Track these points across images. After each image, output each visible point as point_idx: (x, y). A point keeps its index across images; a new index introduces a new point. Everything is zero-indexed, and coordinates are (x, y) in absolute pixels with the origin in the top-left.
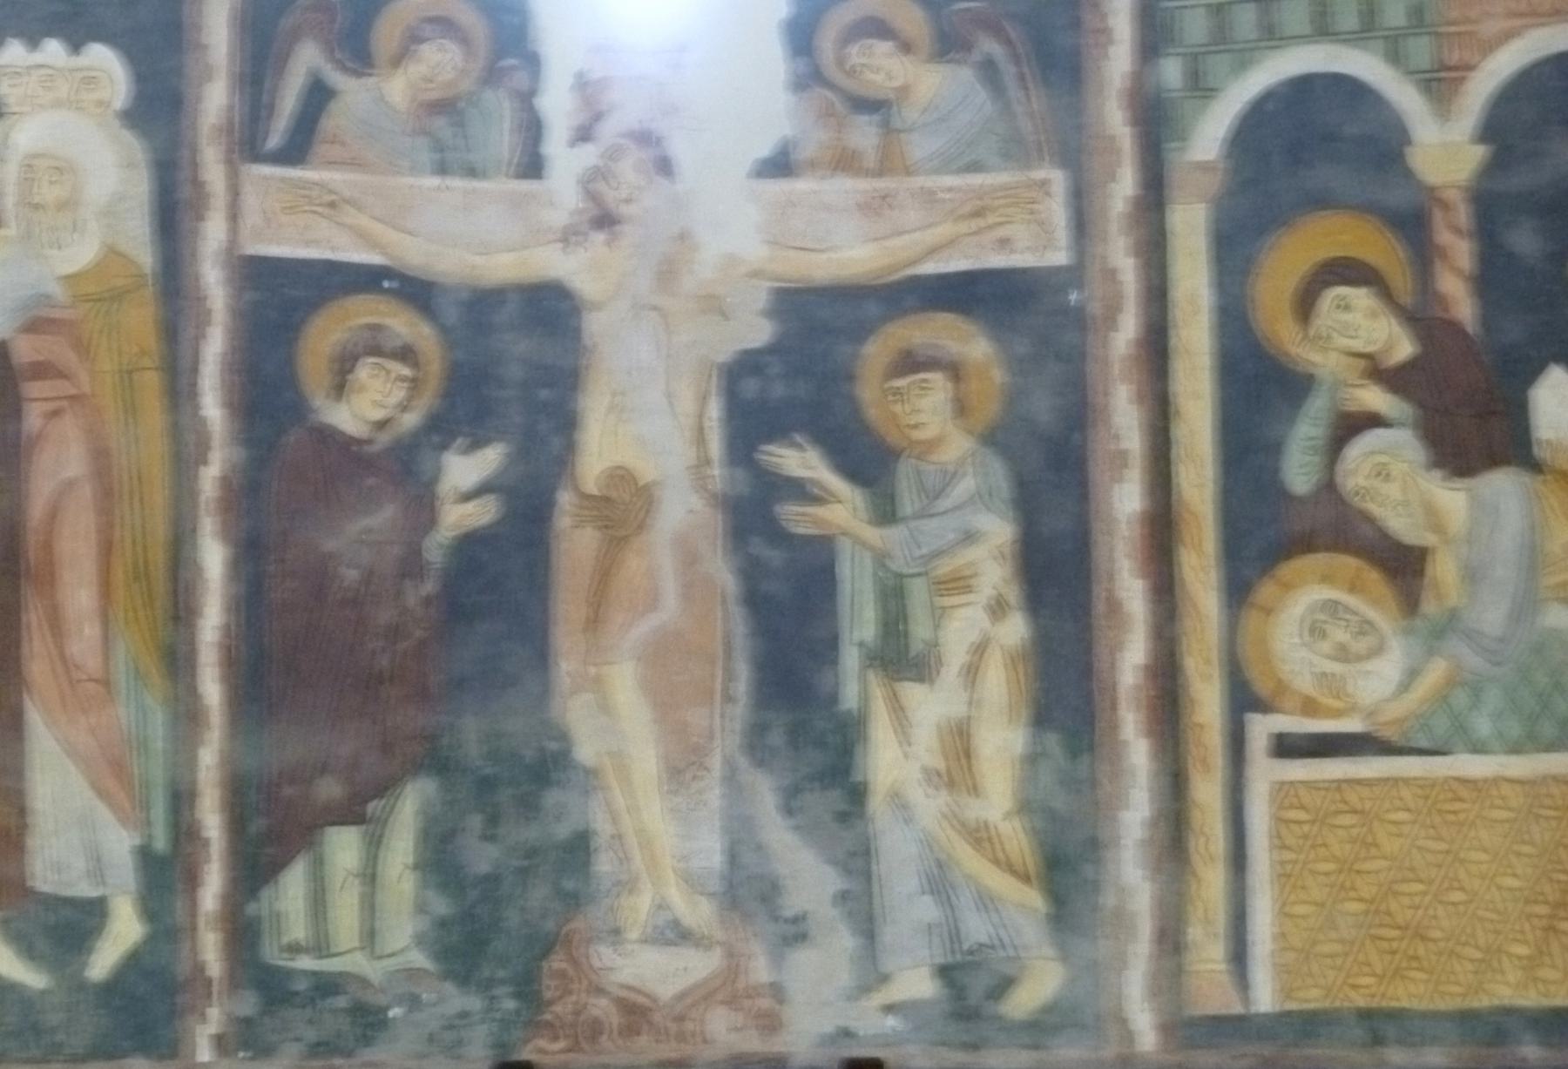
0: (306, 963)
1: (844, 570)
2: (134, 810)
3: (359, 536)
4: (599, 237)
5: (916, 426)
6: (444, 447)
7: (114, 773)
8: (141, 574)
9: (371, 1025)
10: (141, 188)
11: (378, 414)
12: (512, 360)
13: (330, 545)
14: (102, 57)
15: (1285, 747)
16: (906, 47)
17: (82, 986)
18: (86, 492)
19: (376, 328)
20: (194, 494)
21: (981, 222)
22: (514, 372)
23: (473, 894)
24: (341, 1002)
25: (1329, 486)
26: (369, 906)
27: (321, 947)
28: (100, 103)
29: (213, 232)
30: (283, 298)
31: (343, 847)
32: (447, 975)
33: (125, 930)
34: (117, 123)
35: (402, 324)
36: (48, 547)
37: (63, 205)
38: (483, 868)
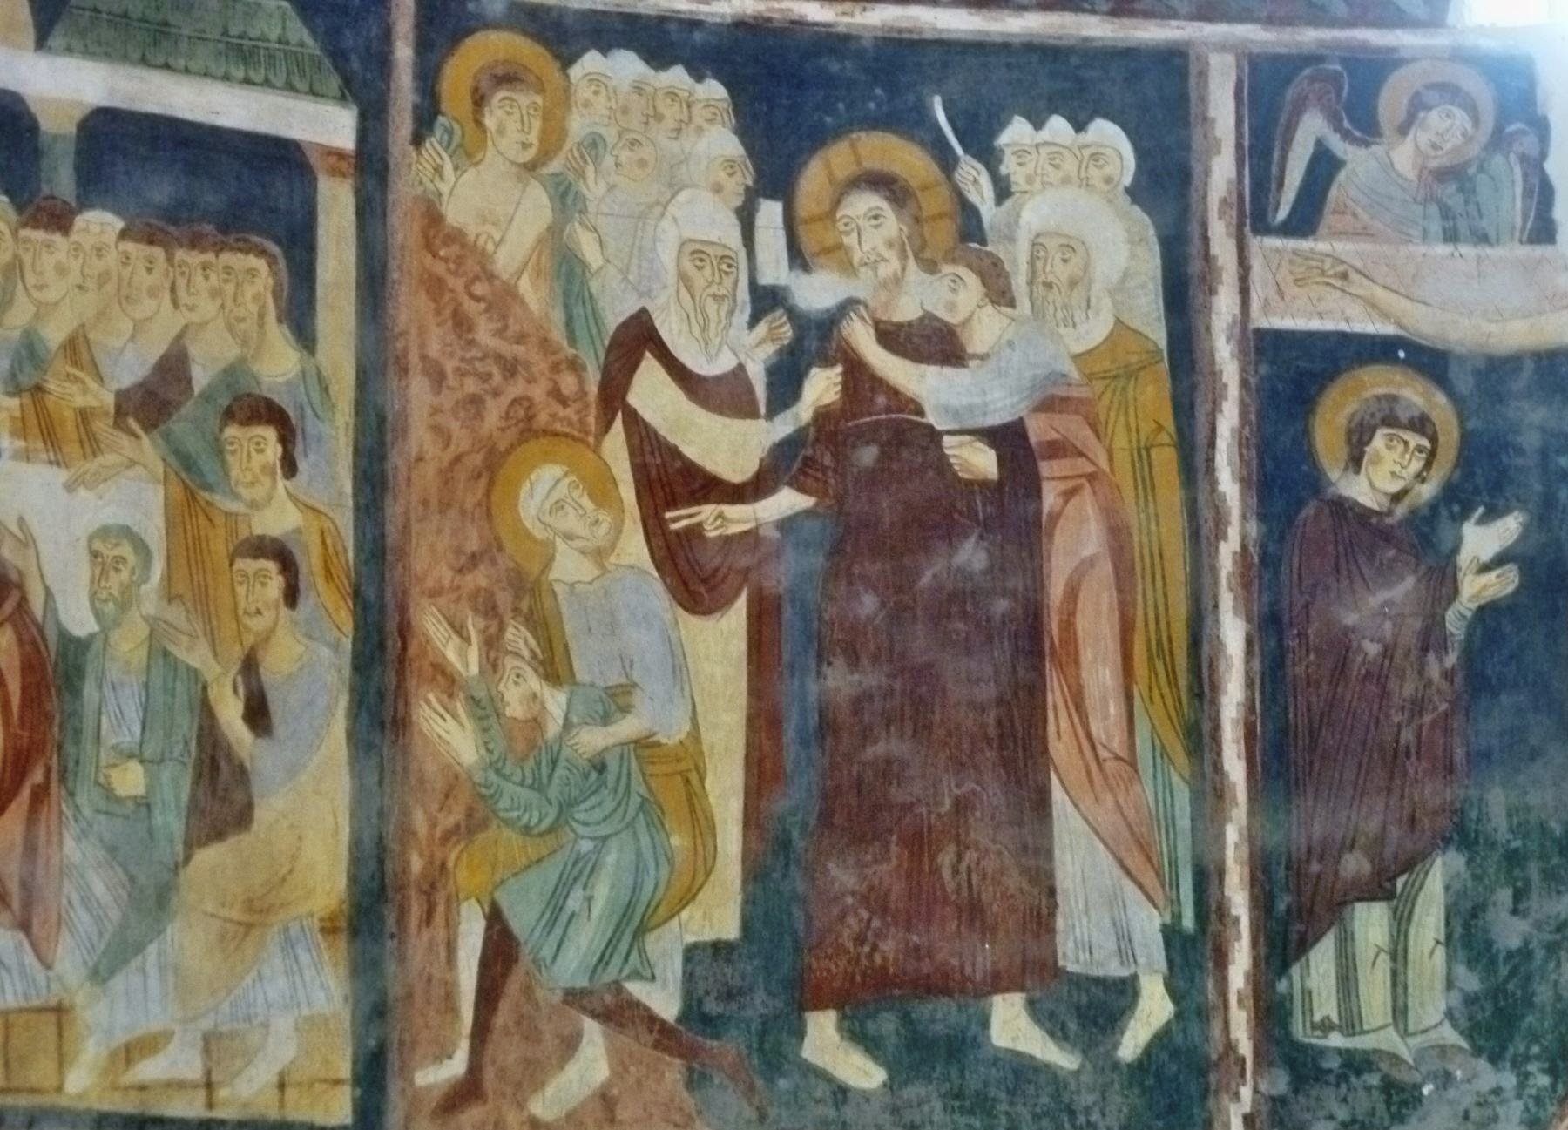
0: (1336, 1040)
2: (1161, 887)
3: (1376, 609)
6: (1464, 515)
7: (1138, 851)
8: (1160, 651)
9: (1404, 1103)
10: (1151, 263)
11: (1394, 487)
13: (1350, 619)
14: (1106, 133)
17: (1116, 1066)
18: (1106, 569)
19: (1393, 399)
20: (1214, 570)
22: (1531, 440)
23: (1504, 971)
24: (1374, 1080)
26: (1398, 981)
27: (1351, 1024)
28: (1108, 180)
29: (1225, 304)
30: (1297, 372)
32: (1477, 1051)
33: (1155, 1007)
34: (1124, 201)
35: (1415, 394)
36: (1068, 625)
37: (1073, 283)
38: (1515, 943)
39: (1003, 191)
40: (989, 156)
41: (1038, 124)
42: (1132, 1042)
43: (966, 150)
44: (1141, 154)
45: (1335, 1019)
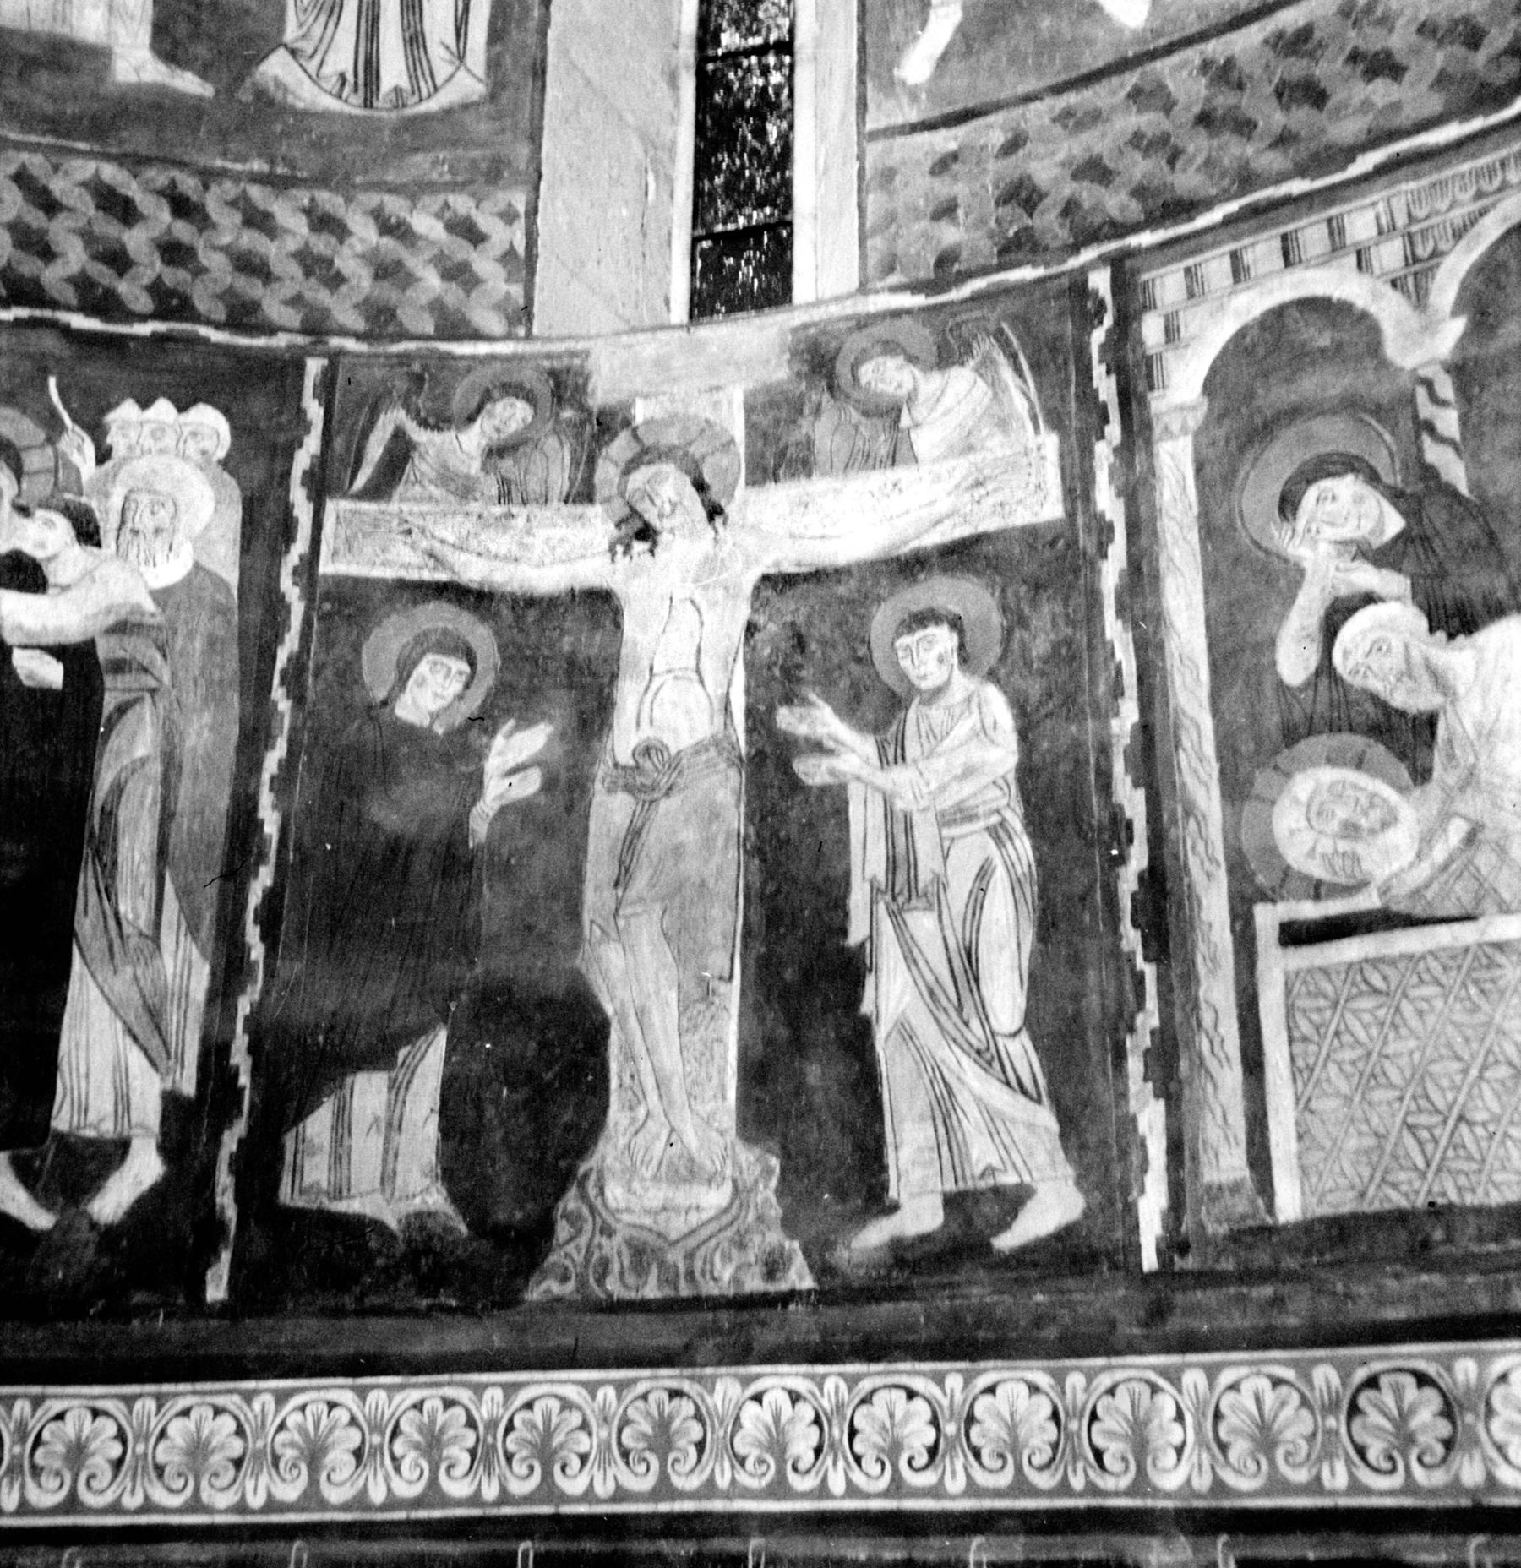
1: (855, 812)
4: (639, 547)
5: (924, 677)
7: (149, 1023)
11: (434, 706)
12: (559, 653)
15: (1295, 935)
16: (912, 359)
18: (156, 769)
21: (982, 491)
25: (1326, 668)
30: (348, 606)
31: (368, 1091)
33: (144, 1168)
36: (109, 815)
39: (103, 455)
40: (96, 430)
41: (145, 404)
42: (113, 1201)
43: (74, 420)
44: (234, 428)
45: (324, 1185)
